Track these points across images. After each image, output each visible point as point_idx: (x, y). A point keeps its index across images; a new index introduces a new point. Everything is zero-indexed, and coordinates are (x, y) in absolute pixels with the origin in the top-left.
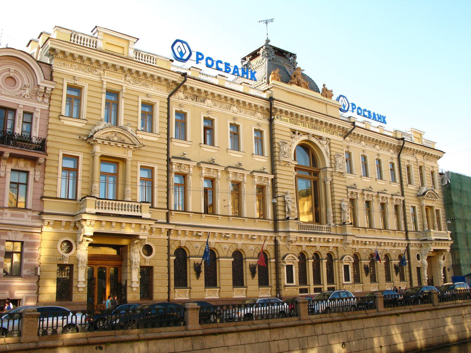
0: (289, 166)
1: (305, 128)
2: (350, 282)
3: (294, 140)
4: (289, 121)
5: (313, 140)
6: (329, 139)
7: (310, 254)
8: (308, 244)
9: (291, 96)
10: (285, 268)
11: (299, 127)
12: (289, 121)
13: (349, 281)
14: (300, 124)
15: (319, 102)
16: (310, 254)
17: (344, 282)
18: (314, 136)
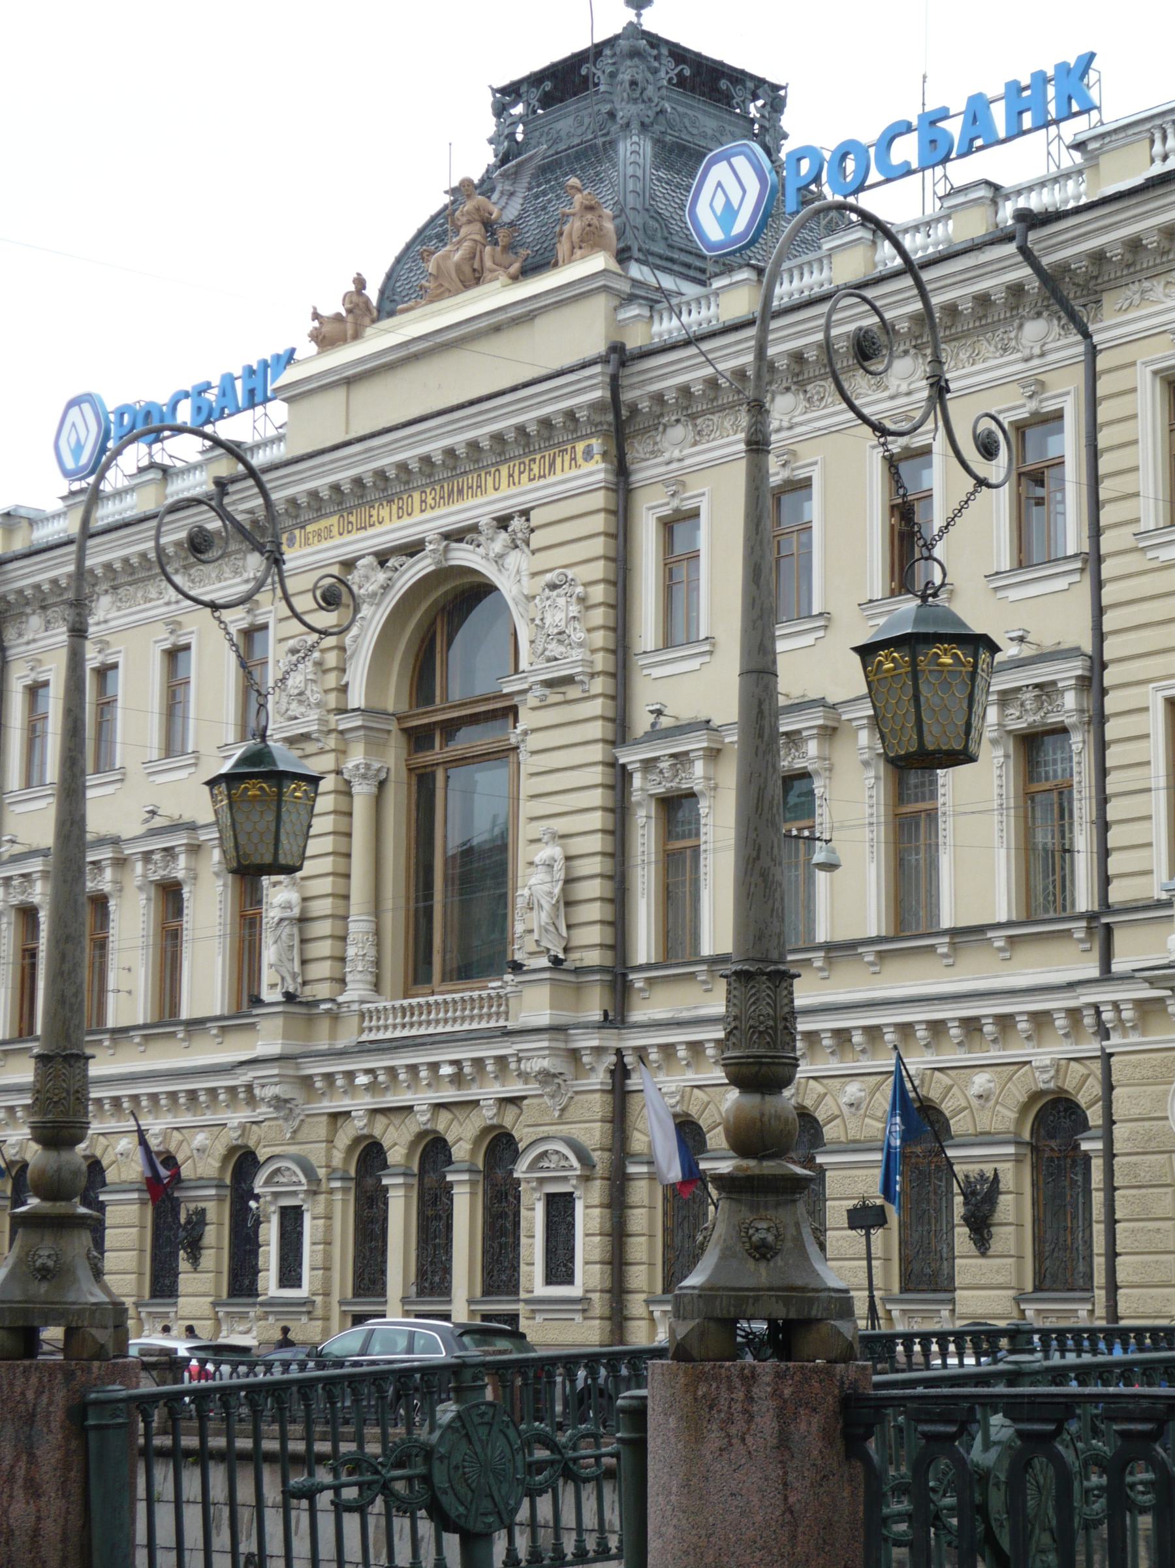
0: (322, 752)
1: (406, 521)
2: (575, 1291)
3: (366, 610)
4: (335, 530)
5: (464, 556)
6: (525, 513)
7: (398, 1144)
8: (367, 1101)
9: (364, 394)
10: (275, 1220)
11: (390, 528)
12: (335, 530)
13: (569, 1279)
14: (384, 512)
15: (497, 329)
16: (398, 1144)
17: (541, 1290)
18: (455, 536)
